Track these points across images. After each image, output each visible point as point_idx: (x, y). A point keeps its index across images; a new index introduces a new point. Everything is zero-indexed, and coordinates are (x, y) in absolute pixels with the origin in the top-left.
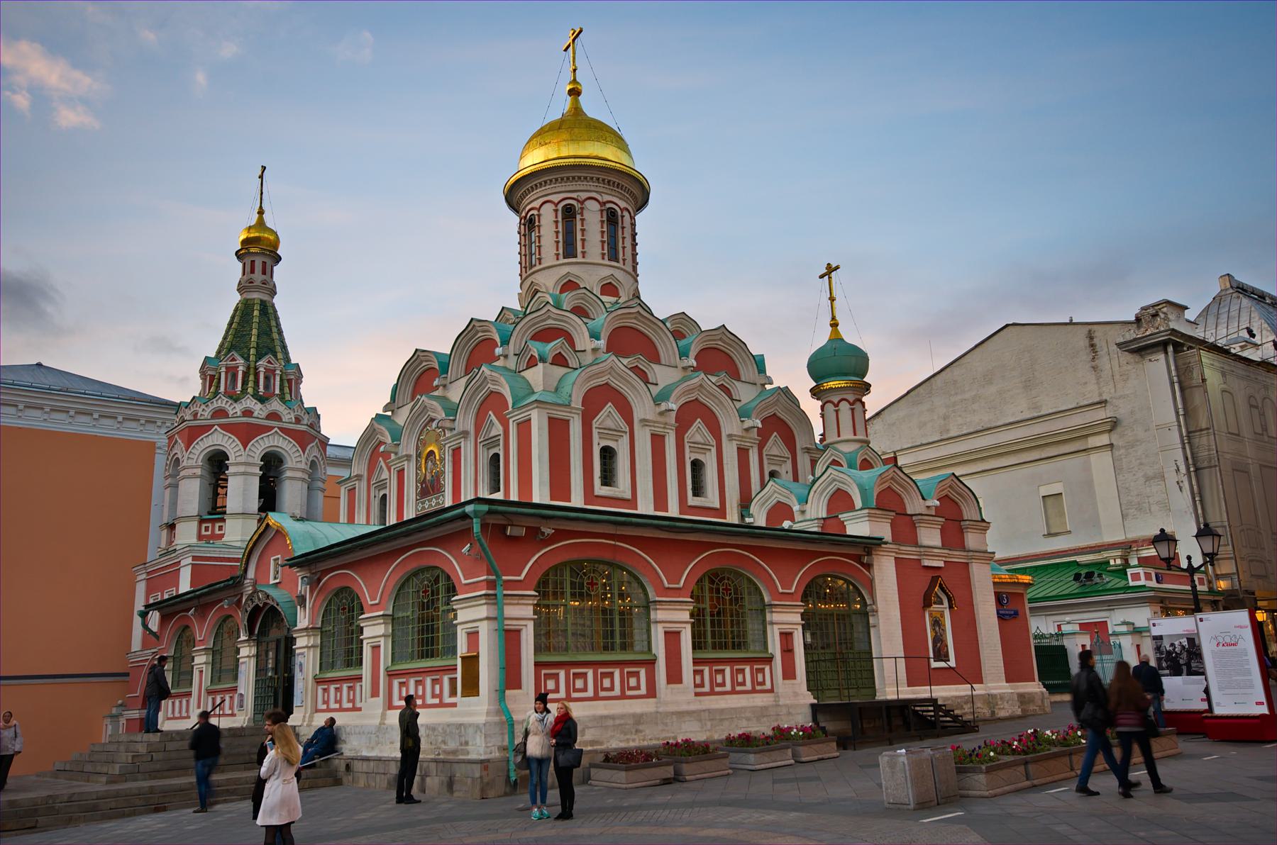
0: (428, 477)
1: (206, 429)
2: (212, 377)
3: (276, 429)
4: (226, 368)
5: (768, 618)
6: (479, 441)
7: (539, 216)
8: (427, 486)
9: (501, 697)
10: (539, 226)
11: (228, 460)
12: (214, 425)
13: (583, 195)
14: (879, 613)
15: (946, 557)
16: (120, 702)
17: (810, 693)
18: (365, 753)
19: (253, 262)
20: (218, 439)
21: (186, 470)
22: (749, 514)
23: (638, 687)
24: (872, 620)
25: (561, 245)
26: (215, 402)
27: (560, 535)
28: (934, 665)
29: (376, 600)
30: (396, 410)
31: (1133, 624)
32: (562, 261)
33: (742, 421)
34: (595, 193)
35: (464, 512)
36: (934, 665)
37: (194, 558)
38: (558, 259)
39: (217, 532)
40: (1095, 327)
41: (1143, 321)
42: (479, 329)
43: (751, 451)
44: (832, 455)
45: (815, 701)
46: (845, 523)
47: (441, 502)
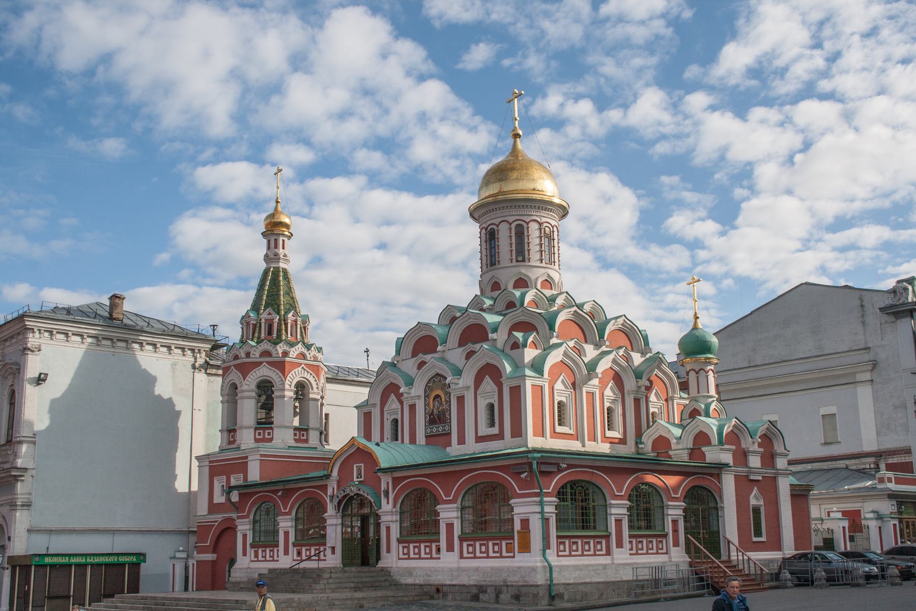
0: (435, 412)
1: (258, 364)
2: (255, 325)
3: (303, 365)
4: (265, 320)
5: (665, 513)
6: (478, 393)
7: (498, 231)
8: (434, 418)
9: (544, 555)
11: (274, 387)
12: (262, 362)
13: (527, 220)
14: (725, 509)
15: (762, 474)
16: (181, 549)
17: (687, 555)
18: (448, 582)
19: (276, 240)
20: (264, 372)
21: (245, 393)
22: (641, 442)
23: (601, 550)
25: (514, 252)
26: (262, 346)
27: (570, 466)
28: (755, 539)
29: (450, 497)
30: (401, 361)
31: (878, 512)
32: (514, 263)
33: (637, 381)
34: (536, 217)
35: (527, 457)
36: (755, 539)
37: (262, 455)
38: (512, 262)
39: (267, 436)
40: (865, 292)
41: (898, 292)
42: (471, 317)
43: (641, 400)
44: (693, 405)
45: (690, 560)
46: (705, 453)
47: (447, 430)
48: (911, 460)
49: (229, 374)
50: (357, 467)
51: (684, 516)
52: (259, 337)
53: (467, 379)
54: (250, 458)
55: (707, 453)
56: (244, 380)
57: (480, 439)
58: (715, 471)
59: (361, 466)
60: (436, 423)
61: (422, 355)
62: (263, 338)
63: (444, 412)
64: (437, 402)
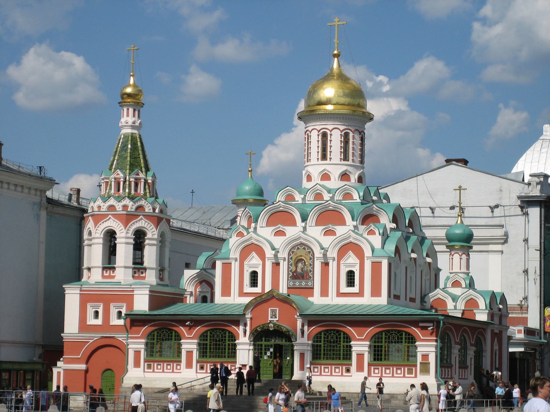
0: (299, 270)
3: (164, 220)
6: (341, 263)
7: (331, 135)
10: (331, 141)
20: (141, 223)
22: (424, 301)
24: (484, 354)
32: (343, 162)
39: (141, 275)
46: (476, 314)
48: (526, 316)
49: (106, 221)
50: (271, 310)
51: (474, 356)
52: (130, 193)
53: (333, 254)
54: (135, 292)
55: (477, 314)
56: (125, 229)
57: (340, 294)
58: (484, 327)
59: (277, 310)
60: (299, 278)
61: (280, 226)
62: (133, 194)
63: (307, 273)
64: (300, 264)
